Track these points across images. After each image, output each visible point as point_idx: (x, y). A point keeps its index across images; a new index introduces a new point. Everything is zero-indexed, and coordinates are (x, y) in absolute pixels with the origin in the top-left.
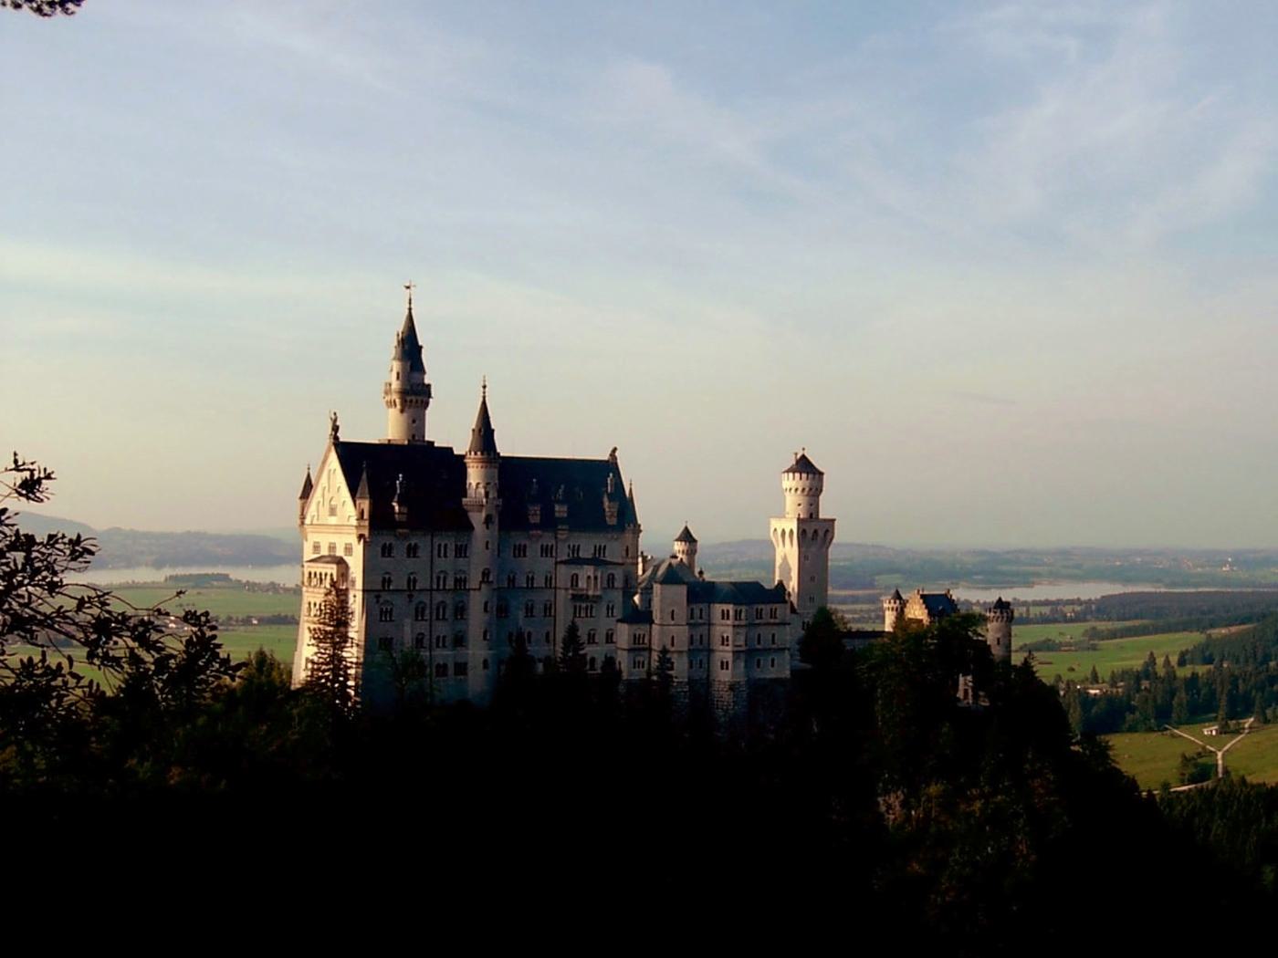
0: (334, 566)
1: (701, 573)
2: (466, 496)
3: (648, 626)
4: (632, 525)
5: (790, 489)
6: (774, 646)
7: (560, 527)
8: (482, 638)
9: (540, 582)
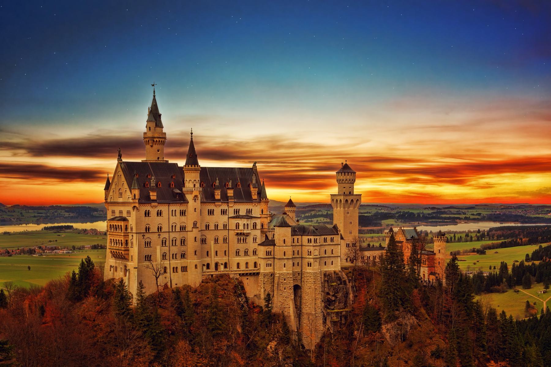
0: (122, 222)
1: (298, 221)
2: (184, 187)
3: (273, 247)
4: (264, 199)
5: (340, 180)
6: (332, 255)
7: (229, 201)
8: (194, 253)
9: (221, 227)
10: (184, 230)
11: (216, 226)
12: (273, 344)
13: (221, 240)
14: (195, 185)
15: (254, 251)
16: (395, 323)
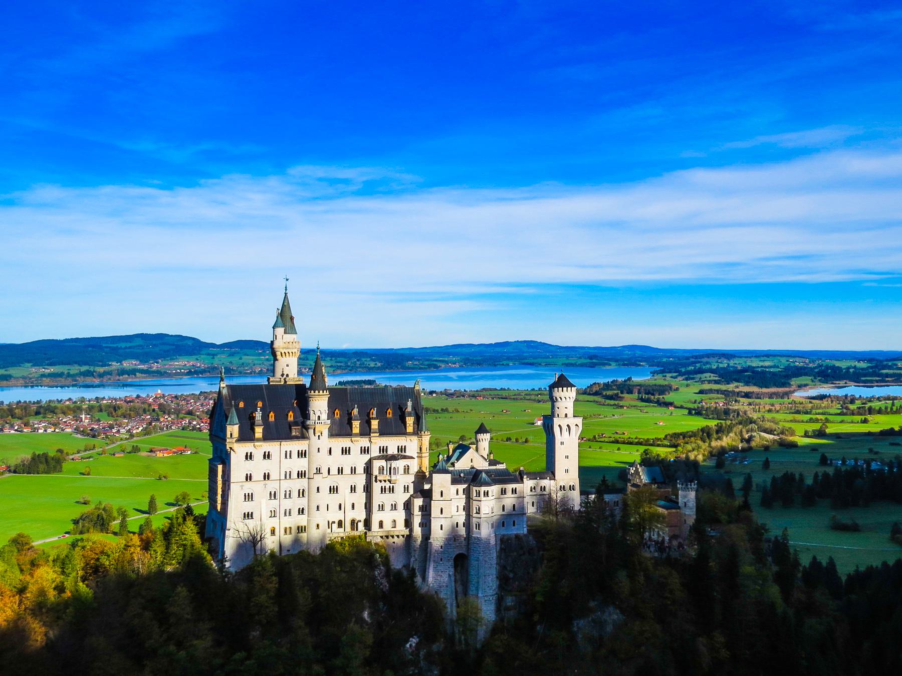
7: (372, 435)
11: (353, 471)
12: (414, 641)
14: (319, 417)
16: (590, 619)
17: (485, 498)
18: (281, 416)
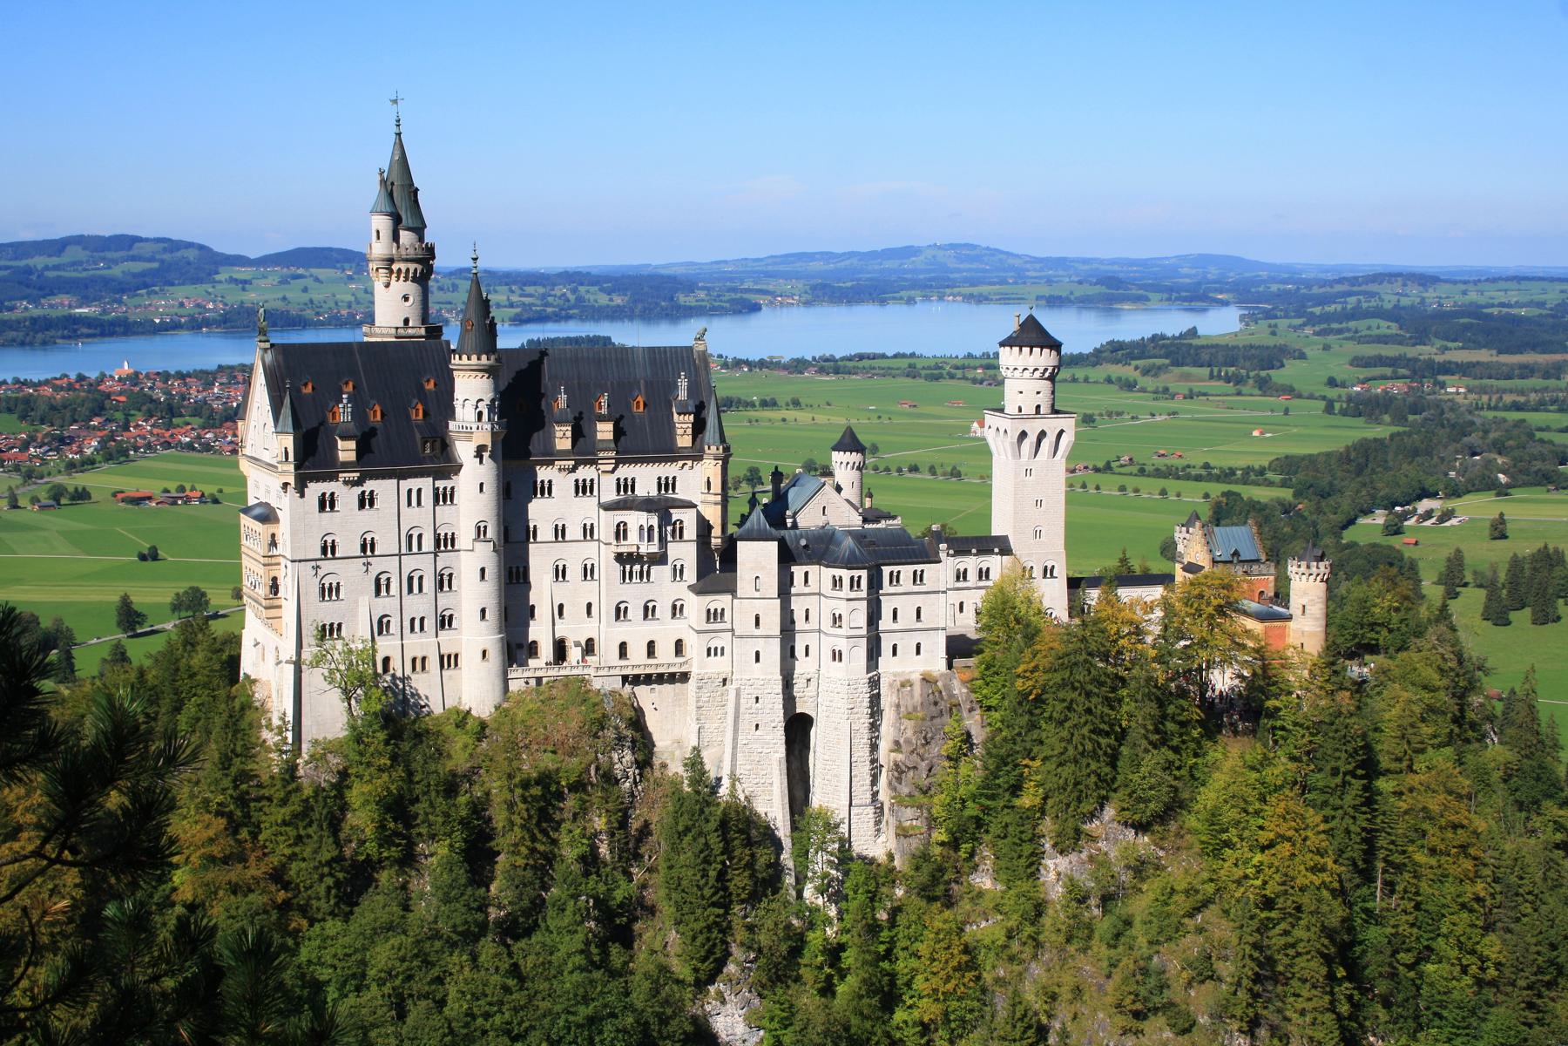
4: (713, 448)
6: (919, 625)
9: (574, 532)
10: (449, 548)
11: (560, 533)
13: (574, 572)
14: (480, 414)
15: (674, 607)
16: (1084, 855)
17: (853, 595)
18: (396, 412)
